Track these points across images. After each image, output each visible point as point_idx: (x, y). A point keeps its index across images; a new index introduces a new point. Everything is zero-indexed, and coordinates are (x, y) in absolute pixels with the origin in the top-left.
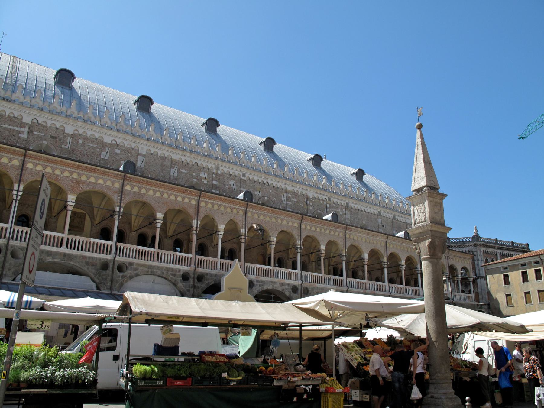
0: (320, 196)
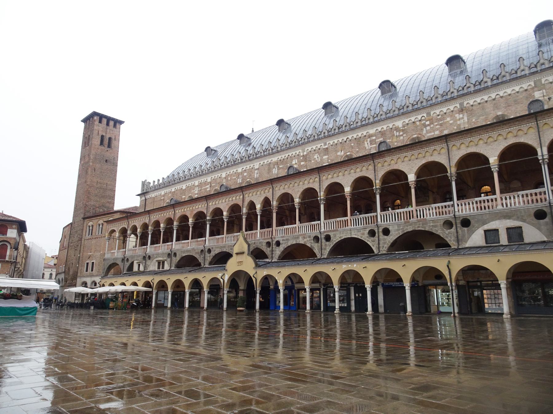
0: (413, 119)
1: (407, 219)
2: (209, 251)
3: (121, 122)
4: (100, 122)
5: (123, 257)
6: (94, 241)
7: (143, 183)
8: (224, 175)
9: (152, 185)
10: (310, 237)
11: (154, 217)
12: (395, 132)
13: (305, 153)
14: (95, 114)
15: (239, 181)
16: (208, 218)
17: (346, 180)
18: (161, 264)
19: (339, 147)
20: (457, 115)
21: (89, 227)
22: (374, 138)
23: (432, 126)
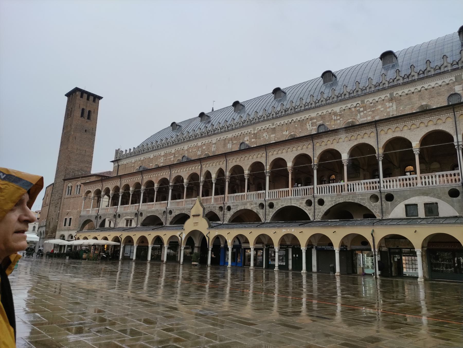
0: (349, 105)
1: (339, 192)
2: (171, 212)
3: (100, 98)
4: (82, 97)
5: (96, 214)
6: (72, 200)
7: (117, 152)
8: (186, 148)
9: (124, 153)
10: (256, 204)
11: (125, 181)
12: (333, 116)
13: (256, 132)
14: (77, 90)
15: (199, 153)
16: (171, 184)
17: (289, 156)
18: (129, 222)
19: (285, 127)
20: (387, 104)
21: (69, 187)
22: (315, 121)
23: (365, 112)
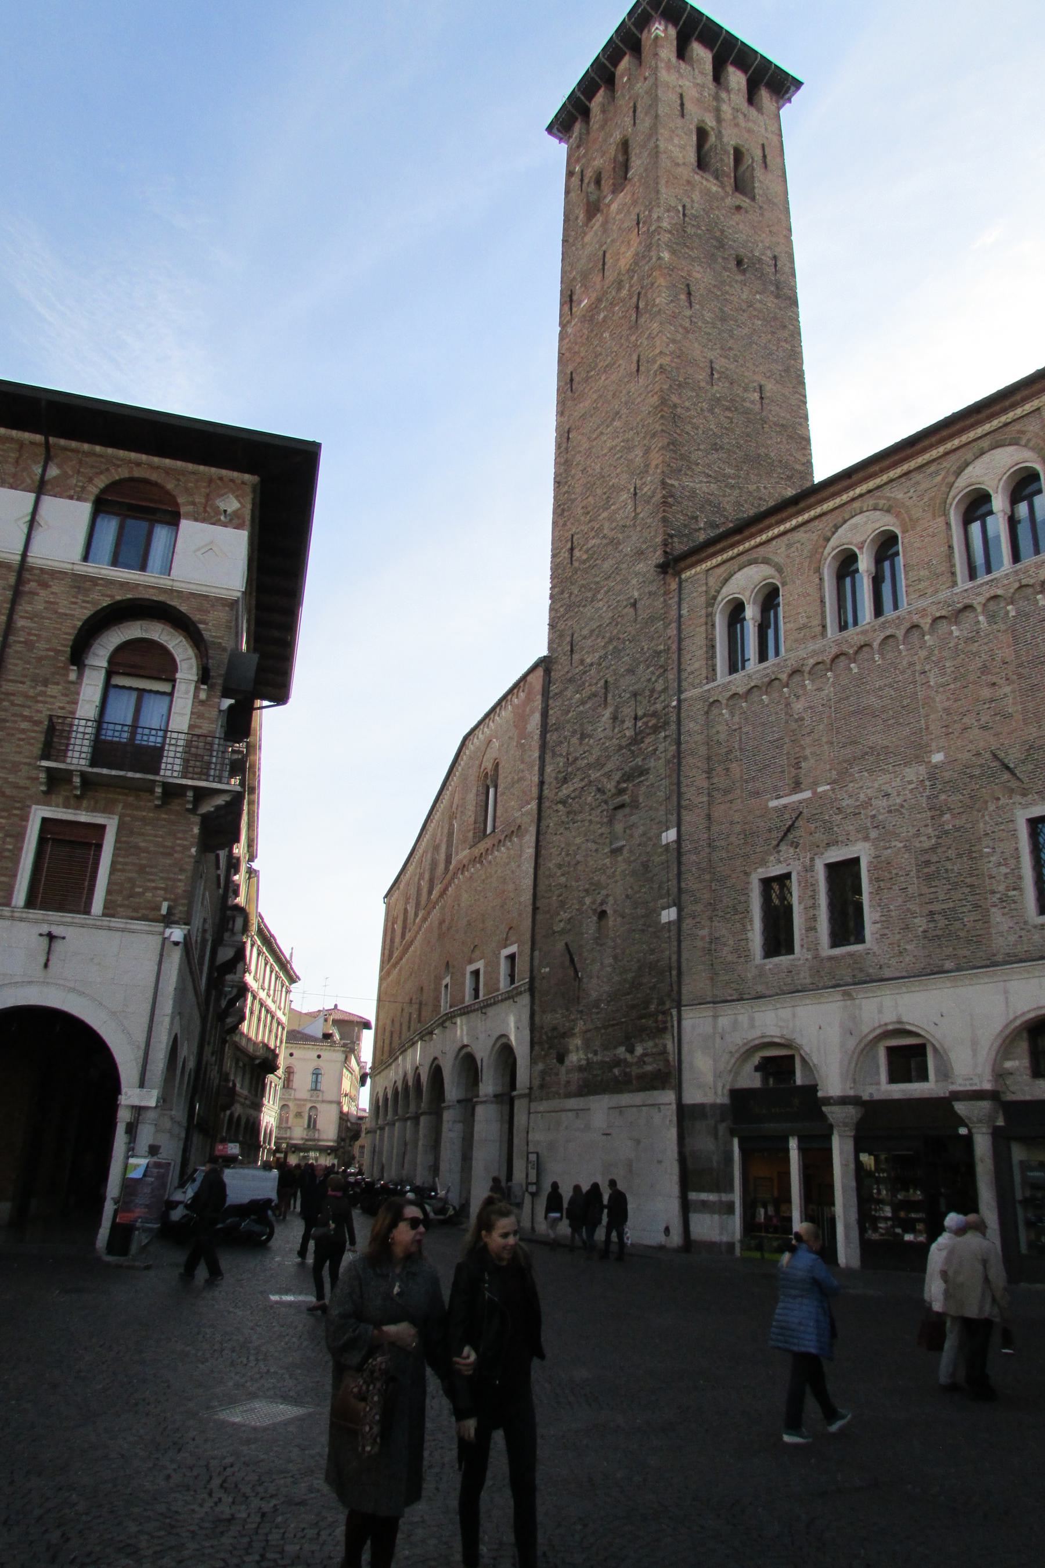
6: (812, 697)
